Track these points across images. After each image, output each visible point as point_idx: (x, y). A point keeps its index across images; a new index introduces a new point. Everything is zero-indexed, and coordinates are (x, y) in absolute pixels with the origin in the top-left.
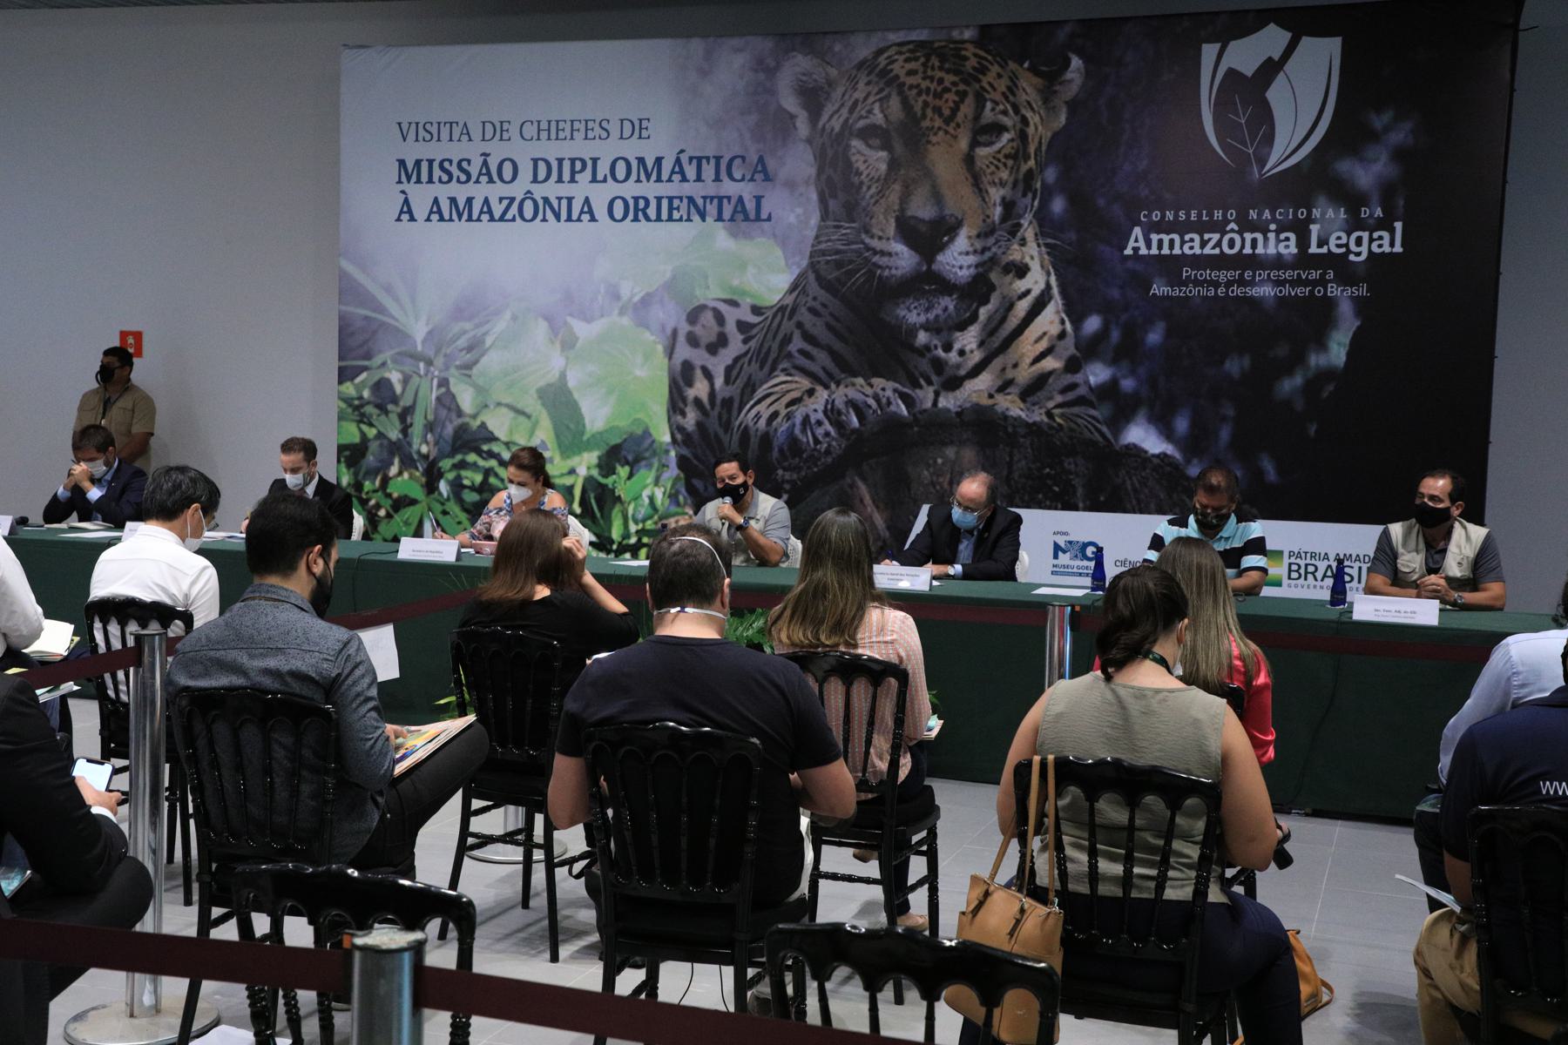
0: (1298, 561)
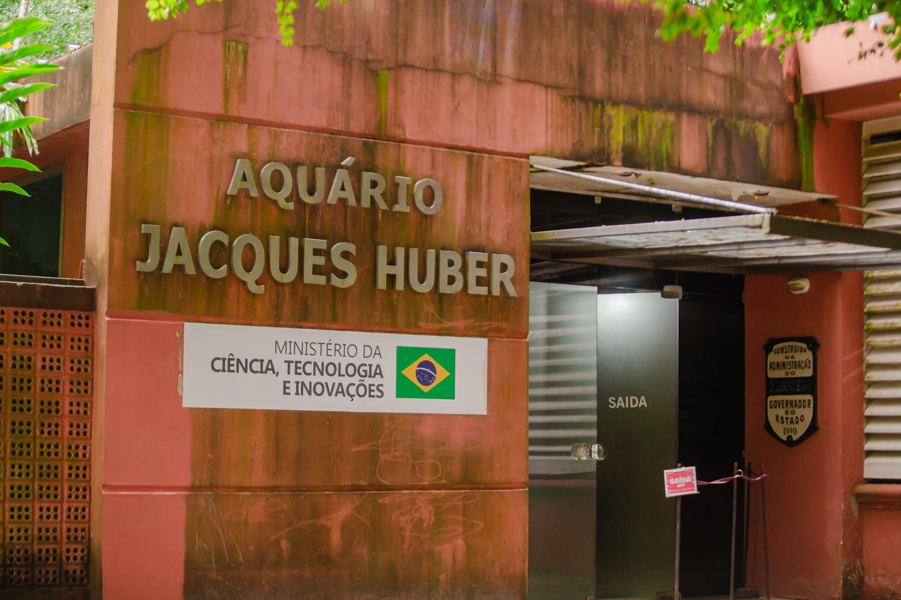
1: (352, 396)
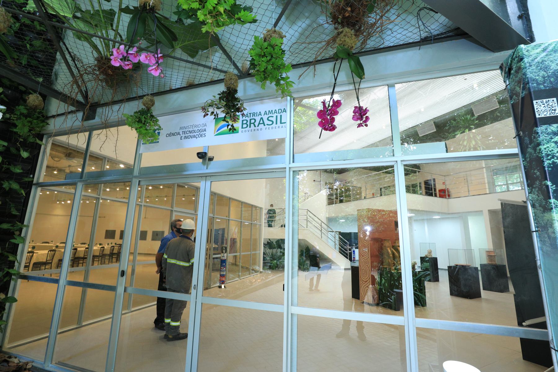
0: (247, 118)
1: (197, 138)
